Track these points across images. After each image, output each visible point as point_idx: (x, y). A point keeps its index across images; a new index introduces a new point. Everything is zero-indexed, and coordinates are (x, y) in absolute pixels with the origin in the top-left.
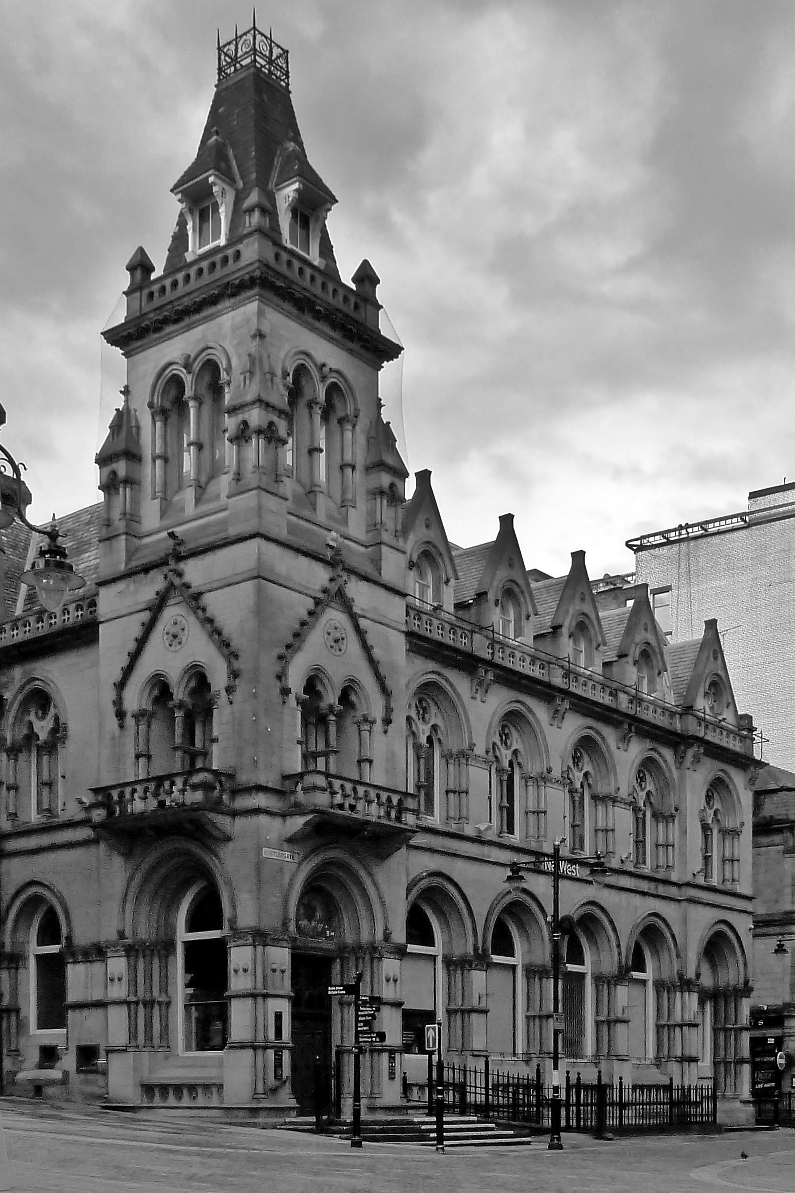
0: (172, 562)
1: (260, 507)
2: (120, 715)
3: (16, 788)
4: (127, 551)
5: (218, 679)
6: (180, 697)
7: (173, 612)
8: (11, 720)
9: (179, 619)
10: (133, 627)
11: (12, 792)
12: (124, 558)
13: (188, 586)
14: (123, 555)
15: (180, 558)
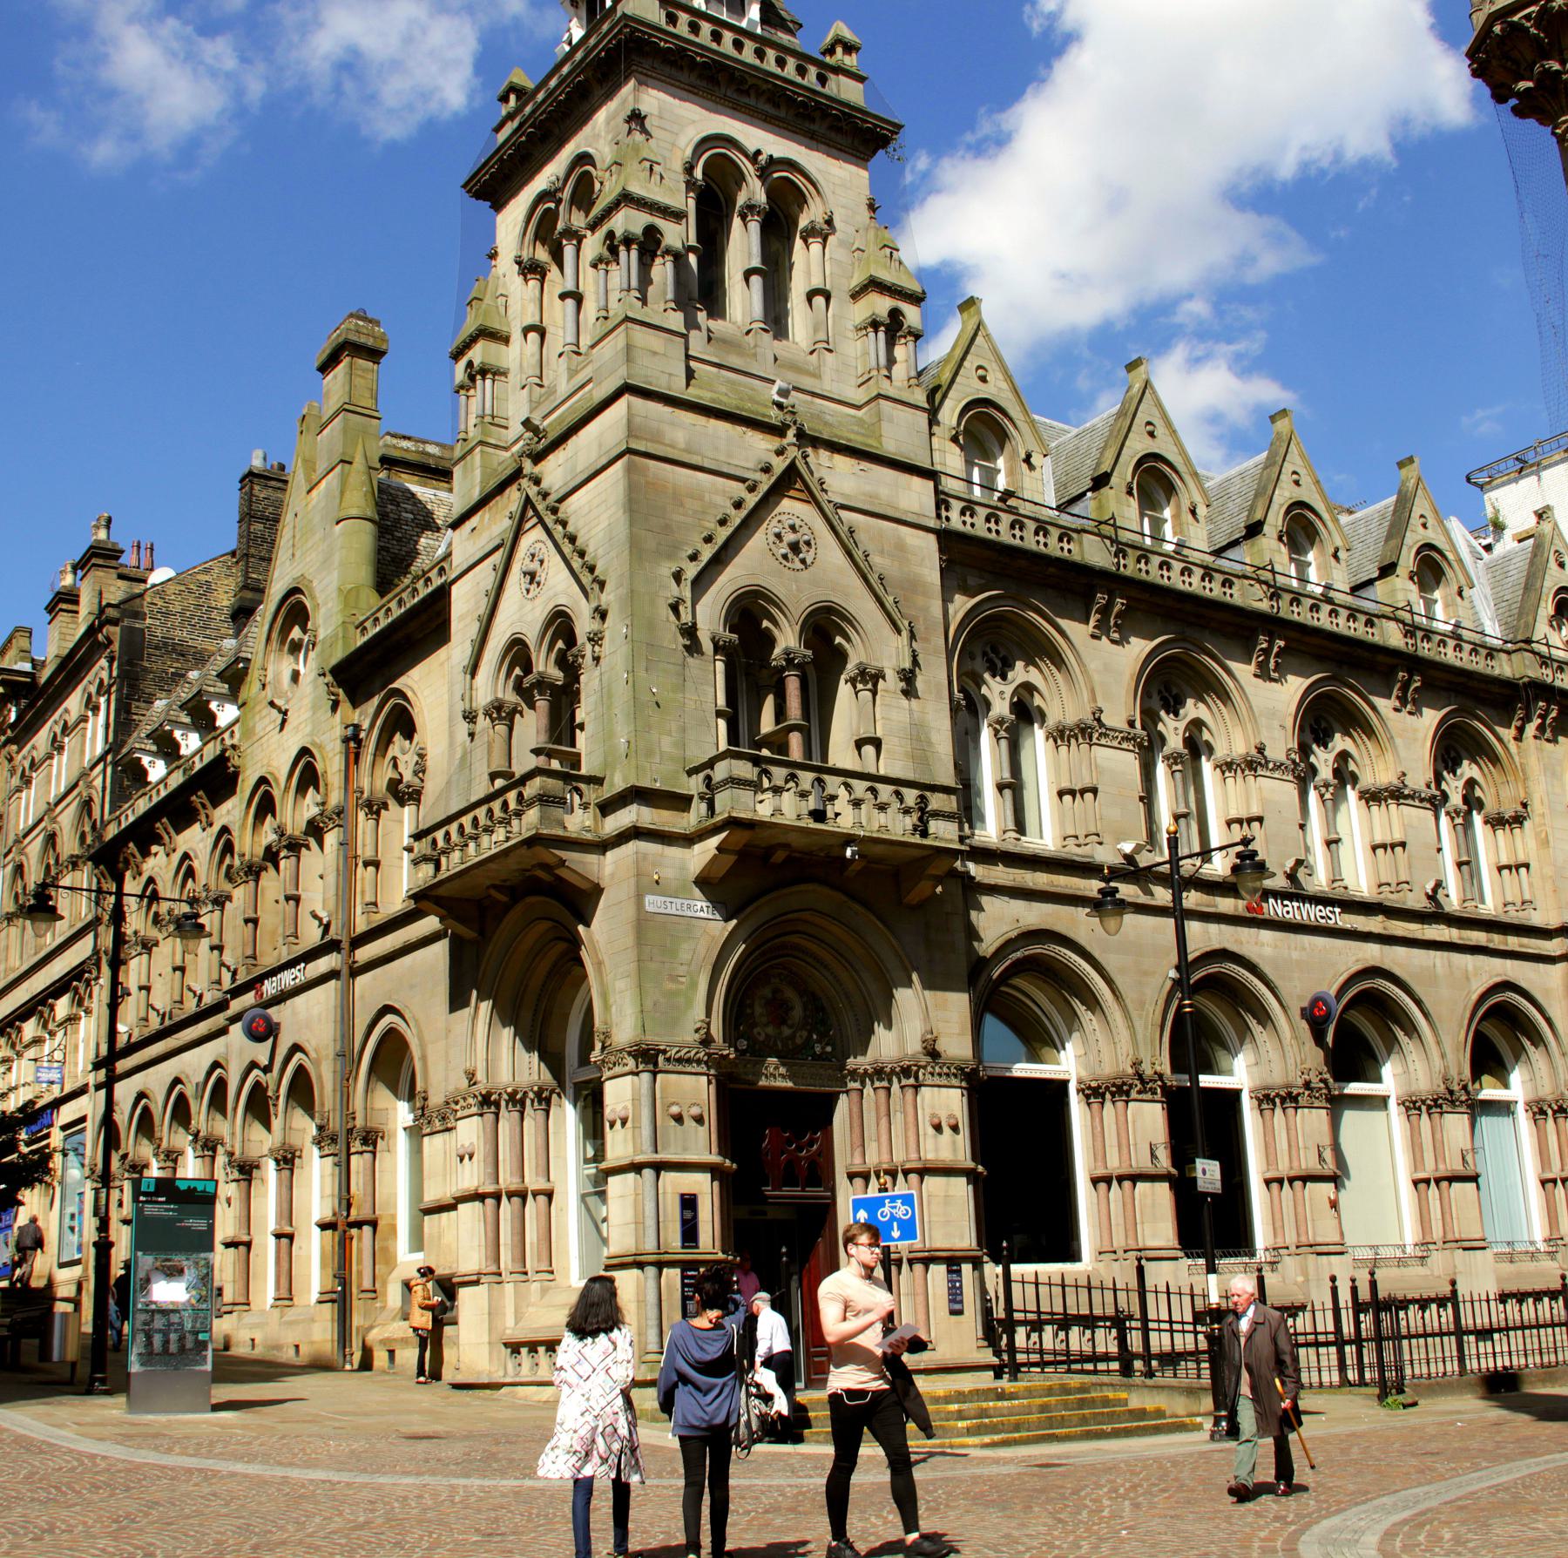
0: (528, 466)
1: (629, 348)
2: (470, 717)
3: (376, 864)
4: (483, 466)
5: (584, 625)
6: (541, 669)
7: (533, 538)
8: (369, 758)
9: (539, 545)
10: (484, 576)
11: (371, 869)
12: (478, 480)
13: (545, 495)
14: (478, 472)
15: (538, 458)
